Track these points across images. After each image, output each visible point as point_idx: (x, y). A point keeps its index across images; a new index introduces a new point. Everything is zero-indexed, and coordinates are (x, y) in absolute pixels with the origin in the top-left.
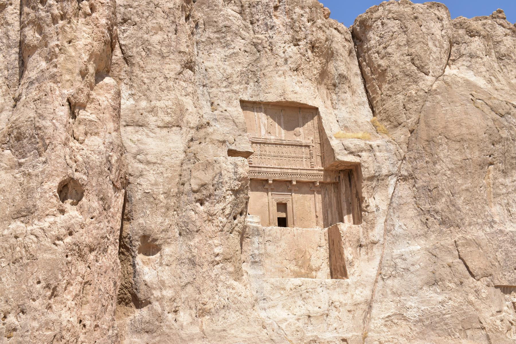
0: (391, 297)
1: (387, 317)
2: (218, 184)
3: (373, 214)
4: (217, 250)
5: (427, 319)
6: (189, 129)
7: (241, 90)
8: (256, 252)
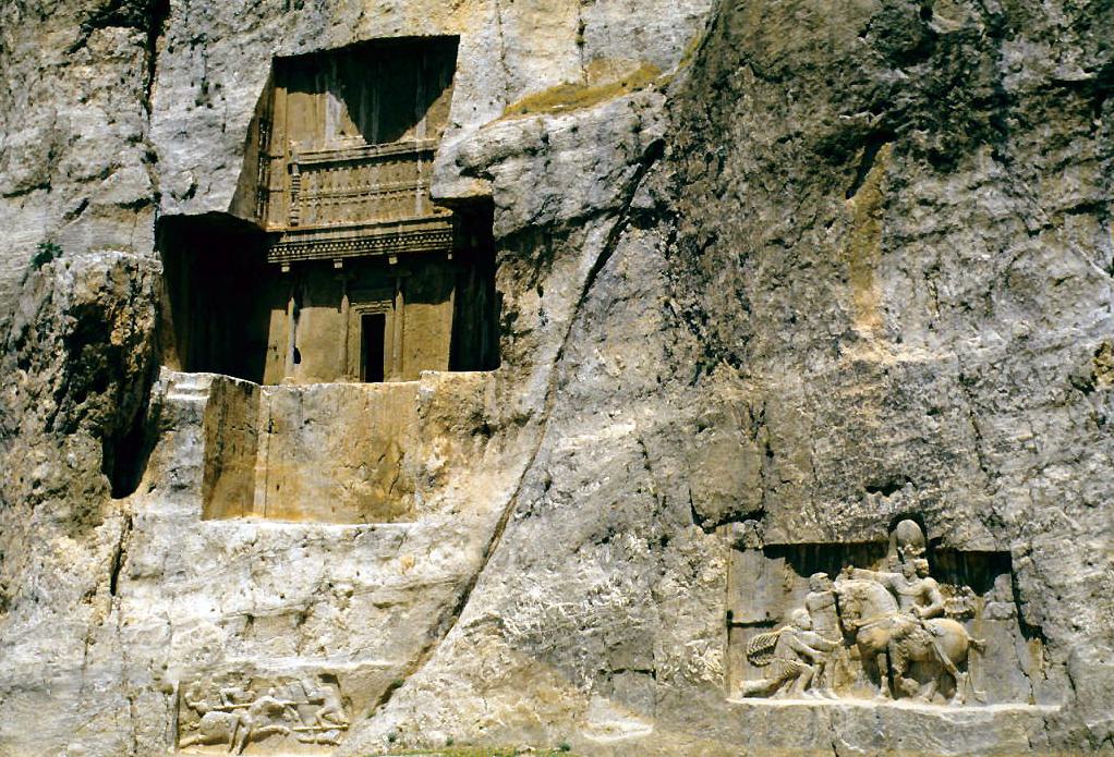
0: (511, 569)
1: (473, 625)
2: (44, 326)
3: (527, 337)
4: (38, 473)
5: (549, 636)
6: (76, 185)
7: (282, 31)
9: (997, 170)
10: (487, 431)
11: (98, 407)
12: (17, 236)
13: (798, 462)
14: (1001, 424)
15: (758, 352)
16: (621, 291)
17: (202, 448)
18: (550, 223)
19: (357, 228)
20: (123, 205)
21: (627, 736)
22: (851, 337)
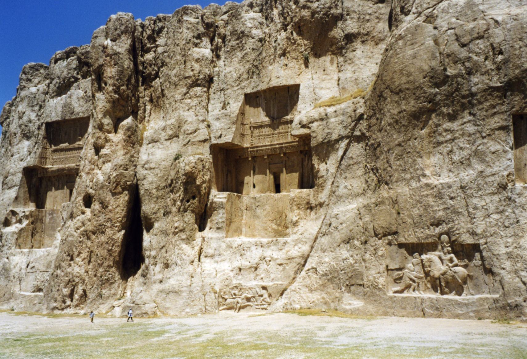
0: (319, 252)
4: (176, 225)
9: (471, 118)
11: (193, 204)
12: (169, 152)
13: (408, 216)
14: (475, 201)
15: (394, 180)
16: (351, 162)
17: (225, 216)
19: (271, 145)
20: (200, 141)
21: (355, 306)
22: (424, 176)
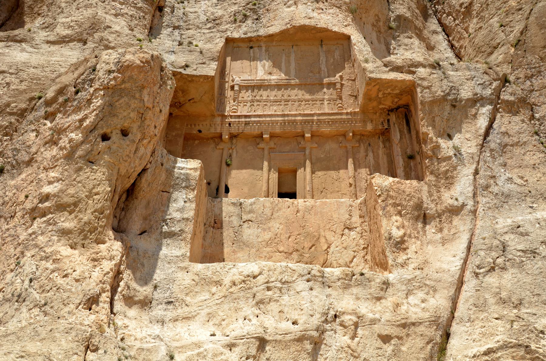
0: (495, 309)
2: (83, 84)
4: (47, 189)
8: (177, 215)
10: (425, 219)
18: (455, 100)
19: (283, 115)
